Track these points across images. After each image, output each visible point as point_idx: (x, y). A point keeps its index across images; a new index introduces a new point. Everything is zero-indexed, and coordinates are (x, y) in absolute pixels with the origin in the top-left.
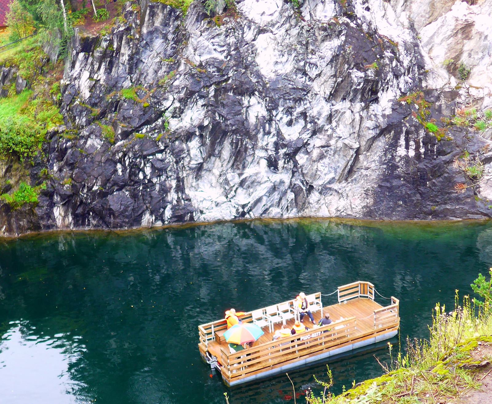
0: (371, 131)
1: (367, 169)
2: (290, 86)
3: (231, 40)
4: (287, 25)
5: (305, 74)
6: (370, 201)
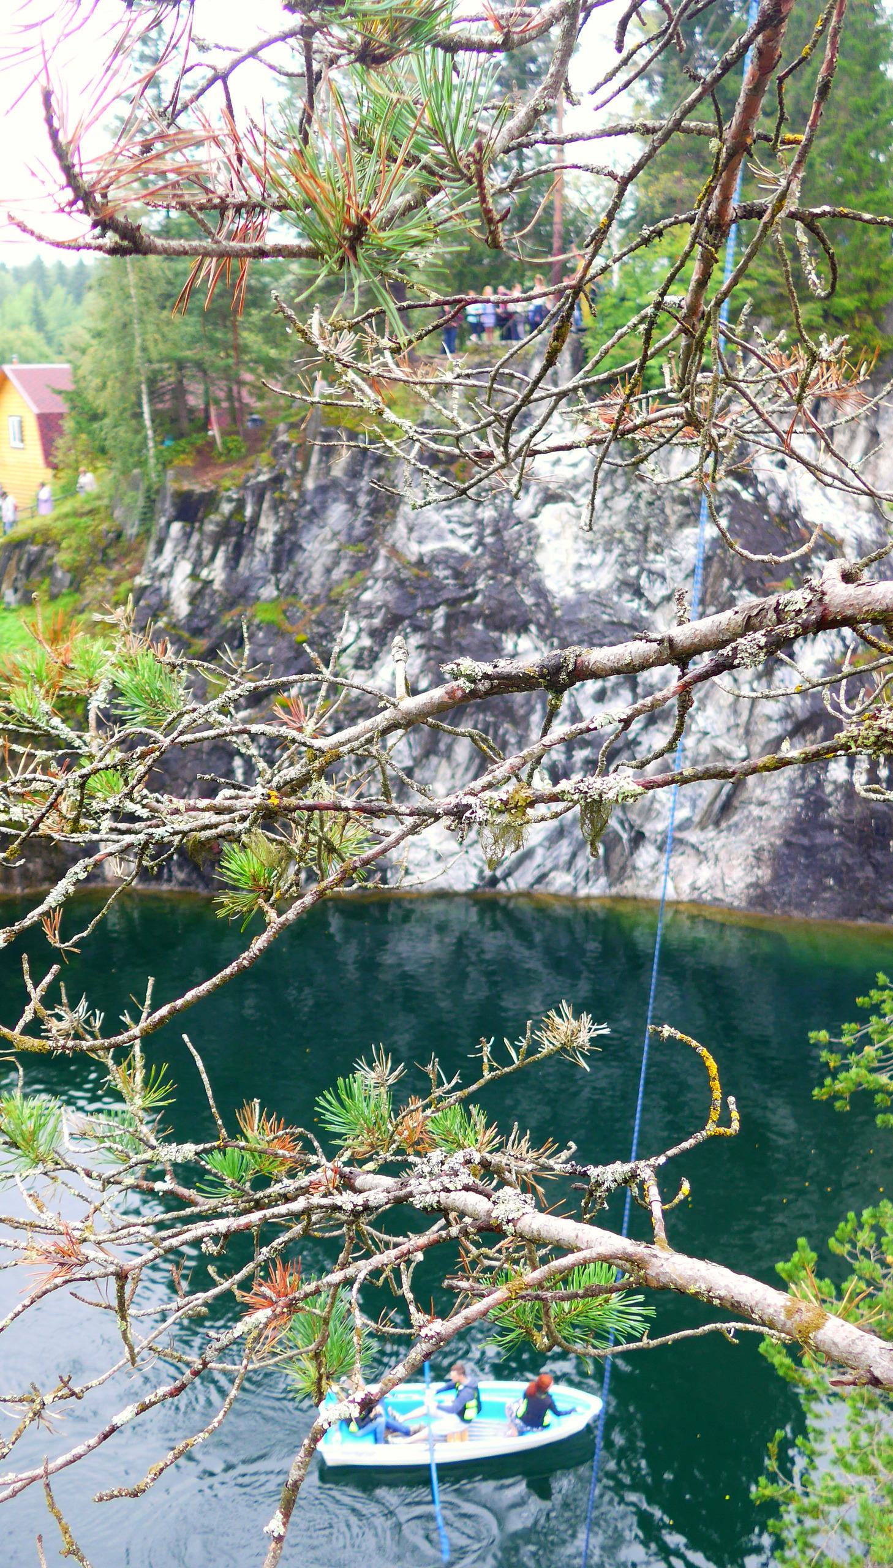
0: (773, 725)
1: (762, 804)
2: (605, 617)
3: (487, 513)
5: (638, 593)
6: (764, 873)
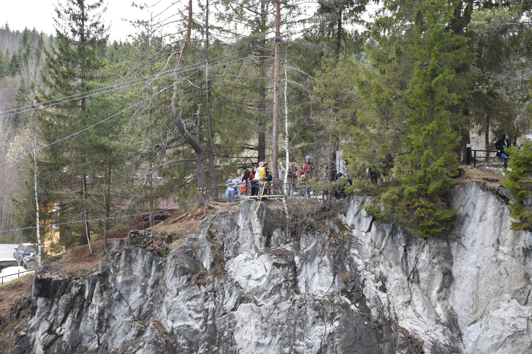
4: (277, 296)
